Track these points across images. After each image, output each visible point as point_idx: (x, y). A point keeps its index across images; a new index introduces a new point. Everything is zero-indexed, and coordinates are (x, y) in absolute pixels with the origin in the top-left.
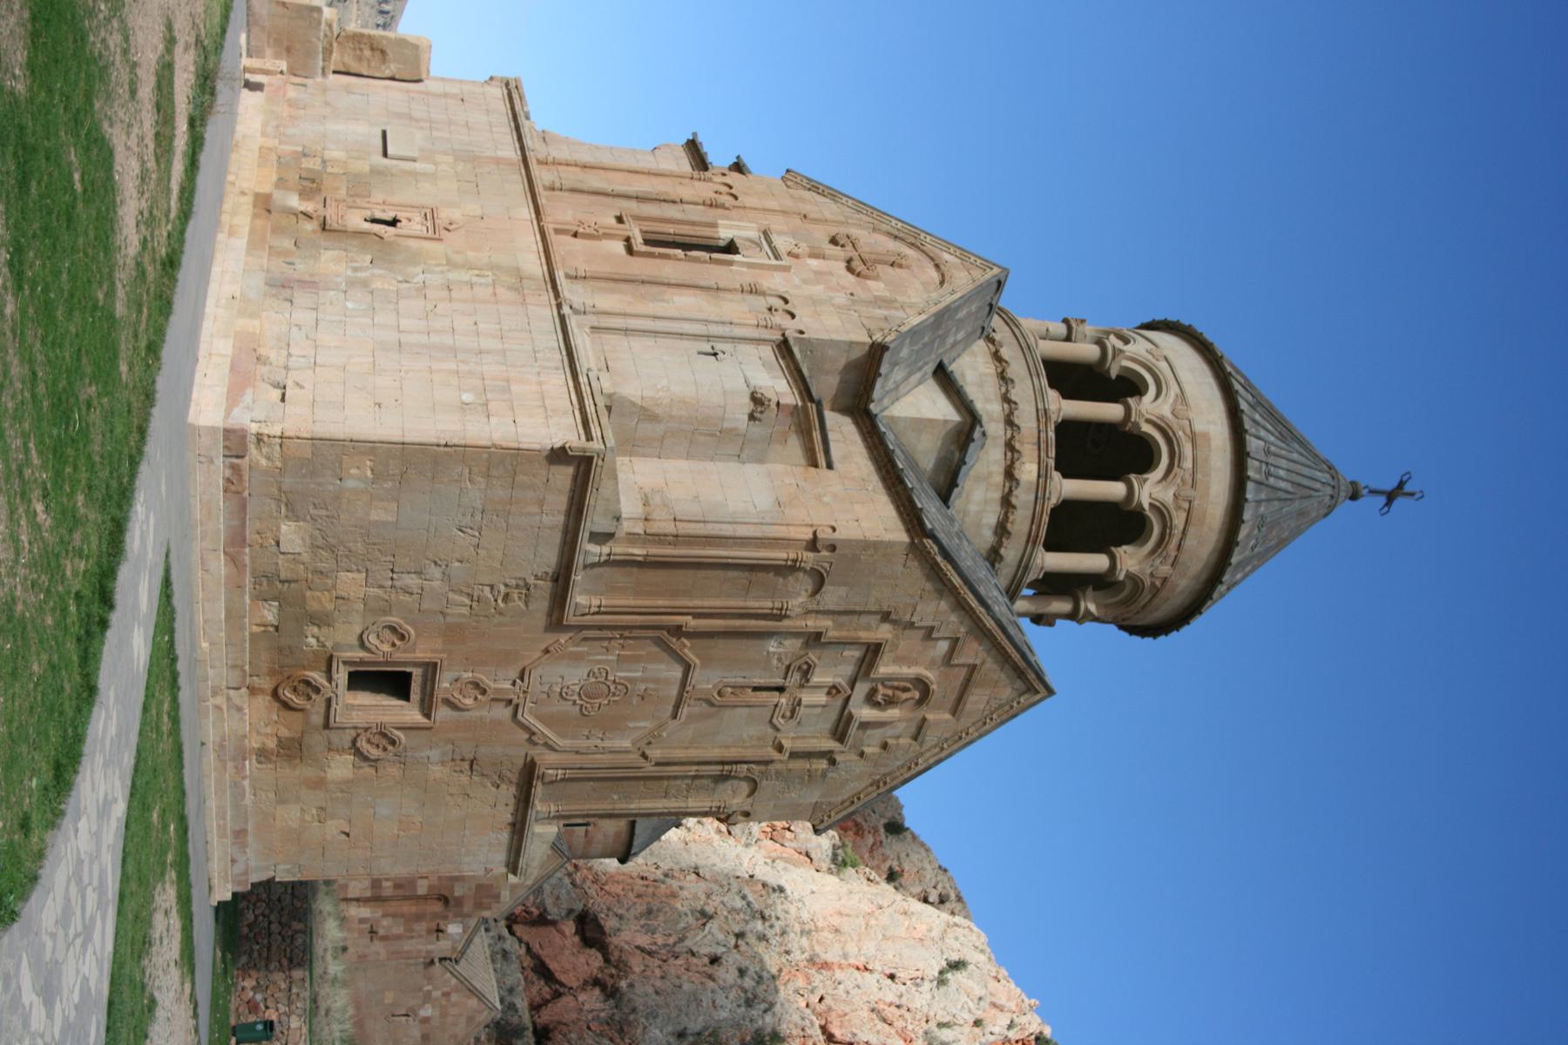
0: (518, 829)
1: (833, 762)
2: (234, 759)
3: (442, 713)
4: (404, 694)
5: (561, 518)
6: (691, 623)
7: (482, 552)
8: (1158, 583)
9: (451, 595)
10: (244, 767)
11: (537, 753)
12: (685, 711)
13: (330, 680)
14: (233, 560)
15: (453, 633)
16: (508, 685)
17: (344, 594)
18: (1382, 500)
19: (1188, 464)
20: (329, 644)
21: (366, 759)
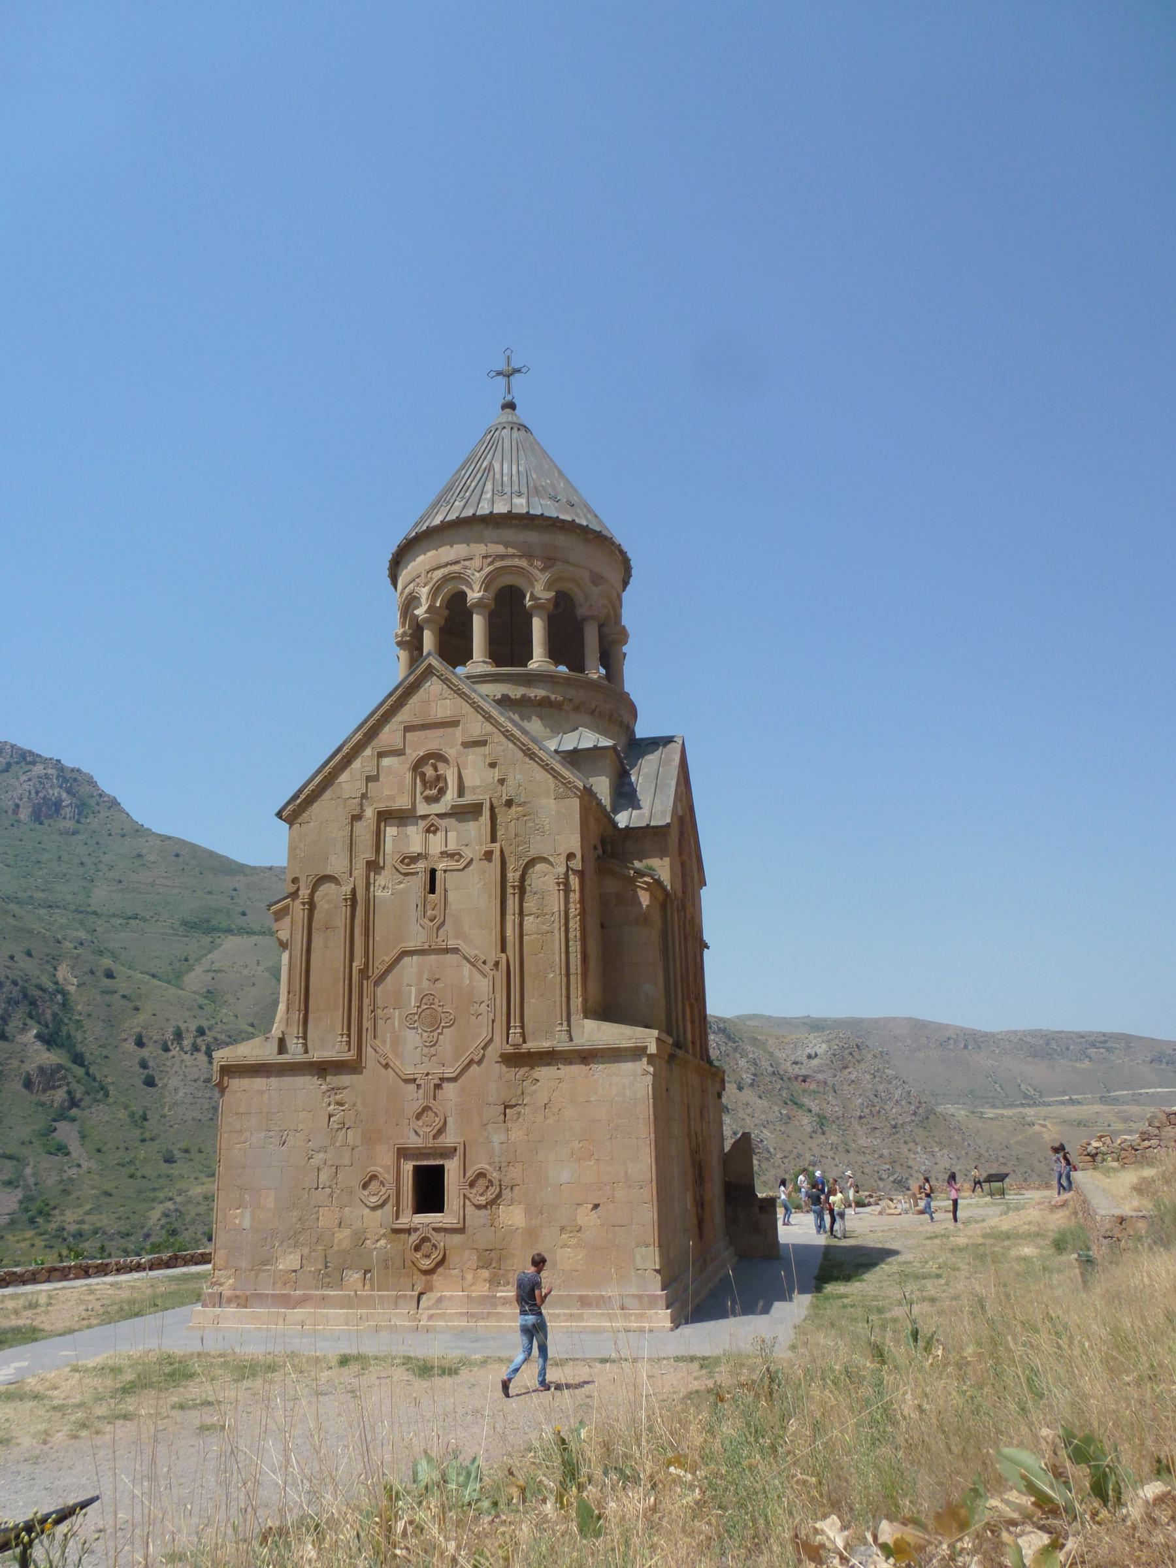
0: (587, 1057)
1: (509, 803)
2: (495, 1306)
3: (450, 1139)
4: (440, 1170)
5: (273, 1079)
6: (357, 964)
7: (301, 1127)
8: (490, 560)
9: (338, 1144)
10: (501, 1297)
11: (493, 1052)
12: (452, 943)
13: (416, 1230)
14: (302, 1301)
15: (370, 1139)
16: (421, 1091)
17: (337, 1221)
18: (515, 378)
19: (412, 585)
20: (383, 1231)
21: (499, 1195)
